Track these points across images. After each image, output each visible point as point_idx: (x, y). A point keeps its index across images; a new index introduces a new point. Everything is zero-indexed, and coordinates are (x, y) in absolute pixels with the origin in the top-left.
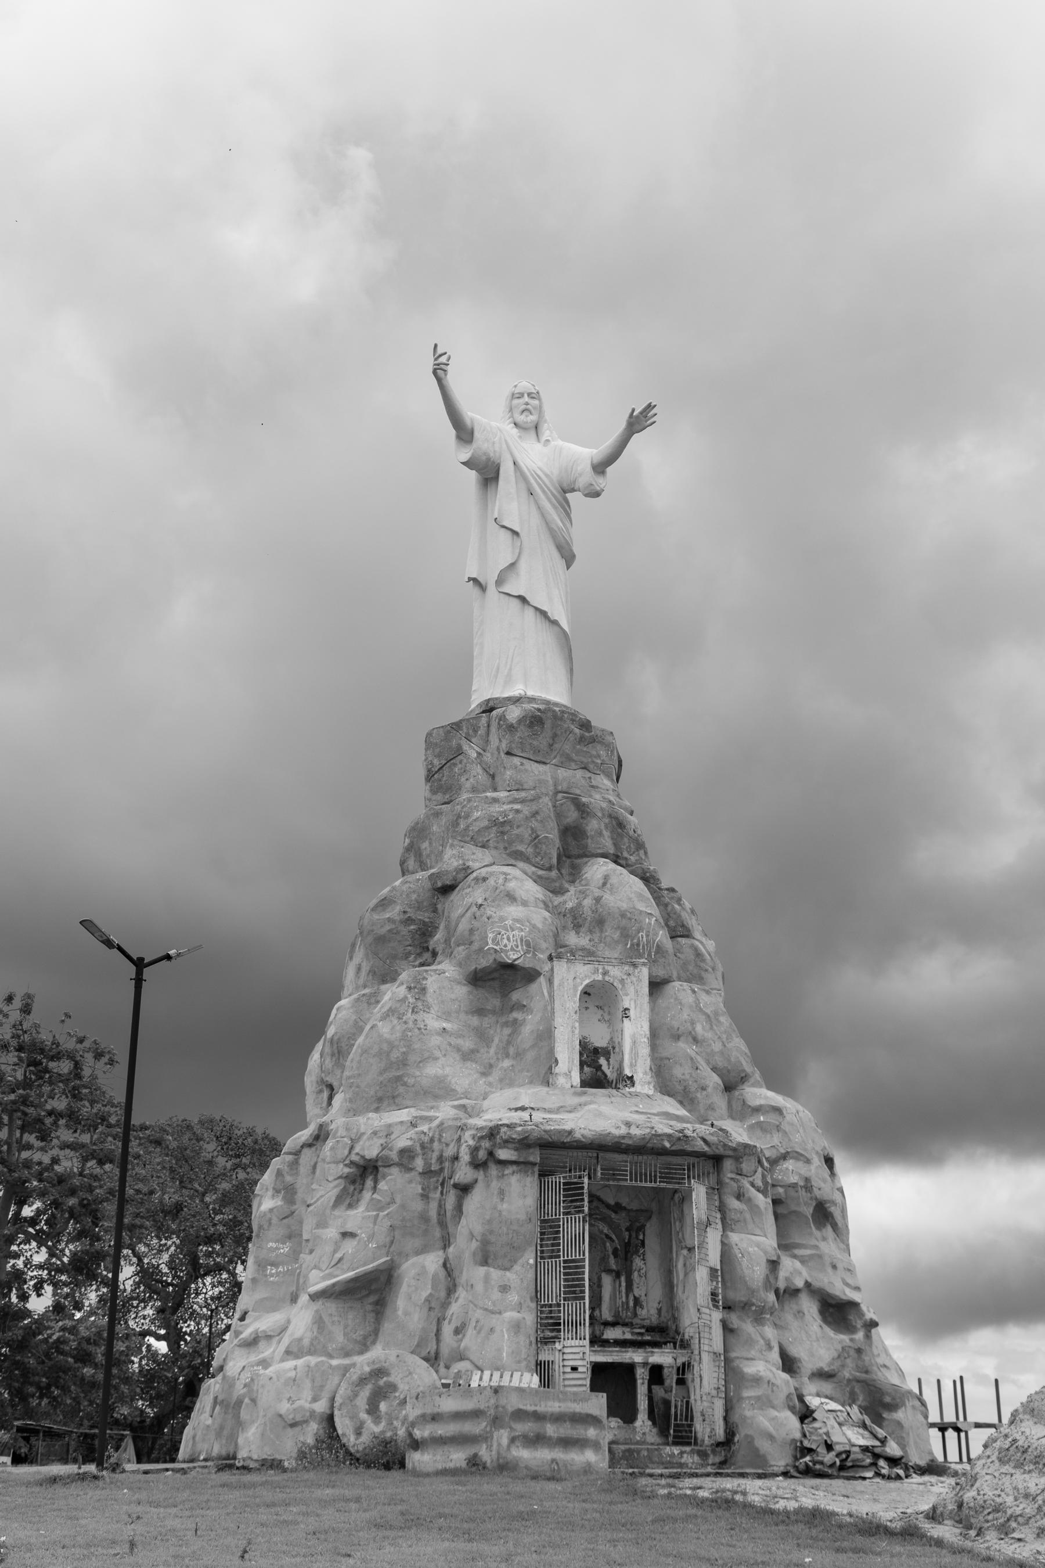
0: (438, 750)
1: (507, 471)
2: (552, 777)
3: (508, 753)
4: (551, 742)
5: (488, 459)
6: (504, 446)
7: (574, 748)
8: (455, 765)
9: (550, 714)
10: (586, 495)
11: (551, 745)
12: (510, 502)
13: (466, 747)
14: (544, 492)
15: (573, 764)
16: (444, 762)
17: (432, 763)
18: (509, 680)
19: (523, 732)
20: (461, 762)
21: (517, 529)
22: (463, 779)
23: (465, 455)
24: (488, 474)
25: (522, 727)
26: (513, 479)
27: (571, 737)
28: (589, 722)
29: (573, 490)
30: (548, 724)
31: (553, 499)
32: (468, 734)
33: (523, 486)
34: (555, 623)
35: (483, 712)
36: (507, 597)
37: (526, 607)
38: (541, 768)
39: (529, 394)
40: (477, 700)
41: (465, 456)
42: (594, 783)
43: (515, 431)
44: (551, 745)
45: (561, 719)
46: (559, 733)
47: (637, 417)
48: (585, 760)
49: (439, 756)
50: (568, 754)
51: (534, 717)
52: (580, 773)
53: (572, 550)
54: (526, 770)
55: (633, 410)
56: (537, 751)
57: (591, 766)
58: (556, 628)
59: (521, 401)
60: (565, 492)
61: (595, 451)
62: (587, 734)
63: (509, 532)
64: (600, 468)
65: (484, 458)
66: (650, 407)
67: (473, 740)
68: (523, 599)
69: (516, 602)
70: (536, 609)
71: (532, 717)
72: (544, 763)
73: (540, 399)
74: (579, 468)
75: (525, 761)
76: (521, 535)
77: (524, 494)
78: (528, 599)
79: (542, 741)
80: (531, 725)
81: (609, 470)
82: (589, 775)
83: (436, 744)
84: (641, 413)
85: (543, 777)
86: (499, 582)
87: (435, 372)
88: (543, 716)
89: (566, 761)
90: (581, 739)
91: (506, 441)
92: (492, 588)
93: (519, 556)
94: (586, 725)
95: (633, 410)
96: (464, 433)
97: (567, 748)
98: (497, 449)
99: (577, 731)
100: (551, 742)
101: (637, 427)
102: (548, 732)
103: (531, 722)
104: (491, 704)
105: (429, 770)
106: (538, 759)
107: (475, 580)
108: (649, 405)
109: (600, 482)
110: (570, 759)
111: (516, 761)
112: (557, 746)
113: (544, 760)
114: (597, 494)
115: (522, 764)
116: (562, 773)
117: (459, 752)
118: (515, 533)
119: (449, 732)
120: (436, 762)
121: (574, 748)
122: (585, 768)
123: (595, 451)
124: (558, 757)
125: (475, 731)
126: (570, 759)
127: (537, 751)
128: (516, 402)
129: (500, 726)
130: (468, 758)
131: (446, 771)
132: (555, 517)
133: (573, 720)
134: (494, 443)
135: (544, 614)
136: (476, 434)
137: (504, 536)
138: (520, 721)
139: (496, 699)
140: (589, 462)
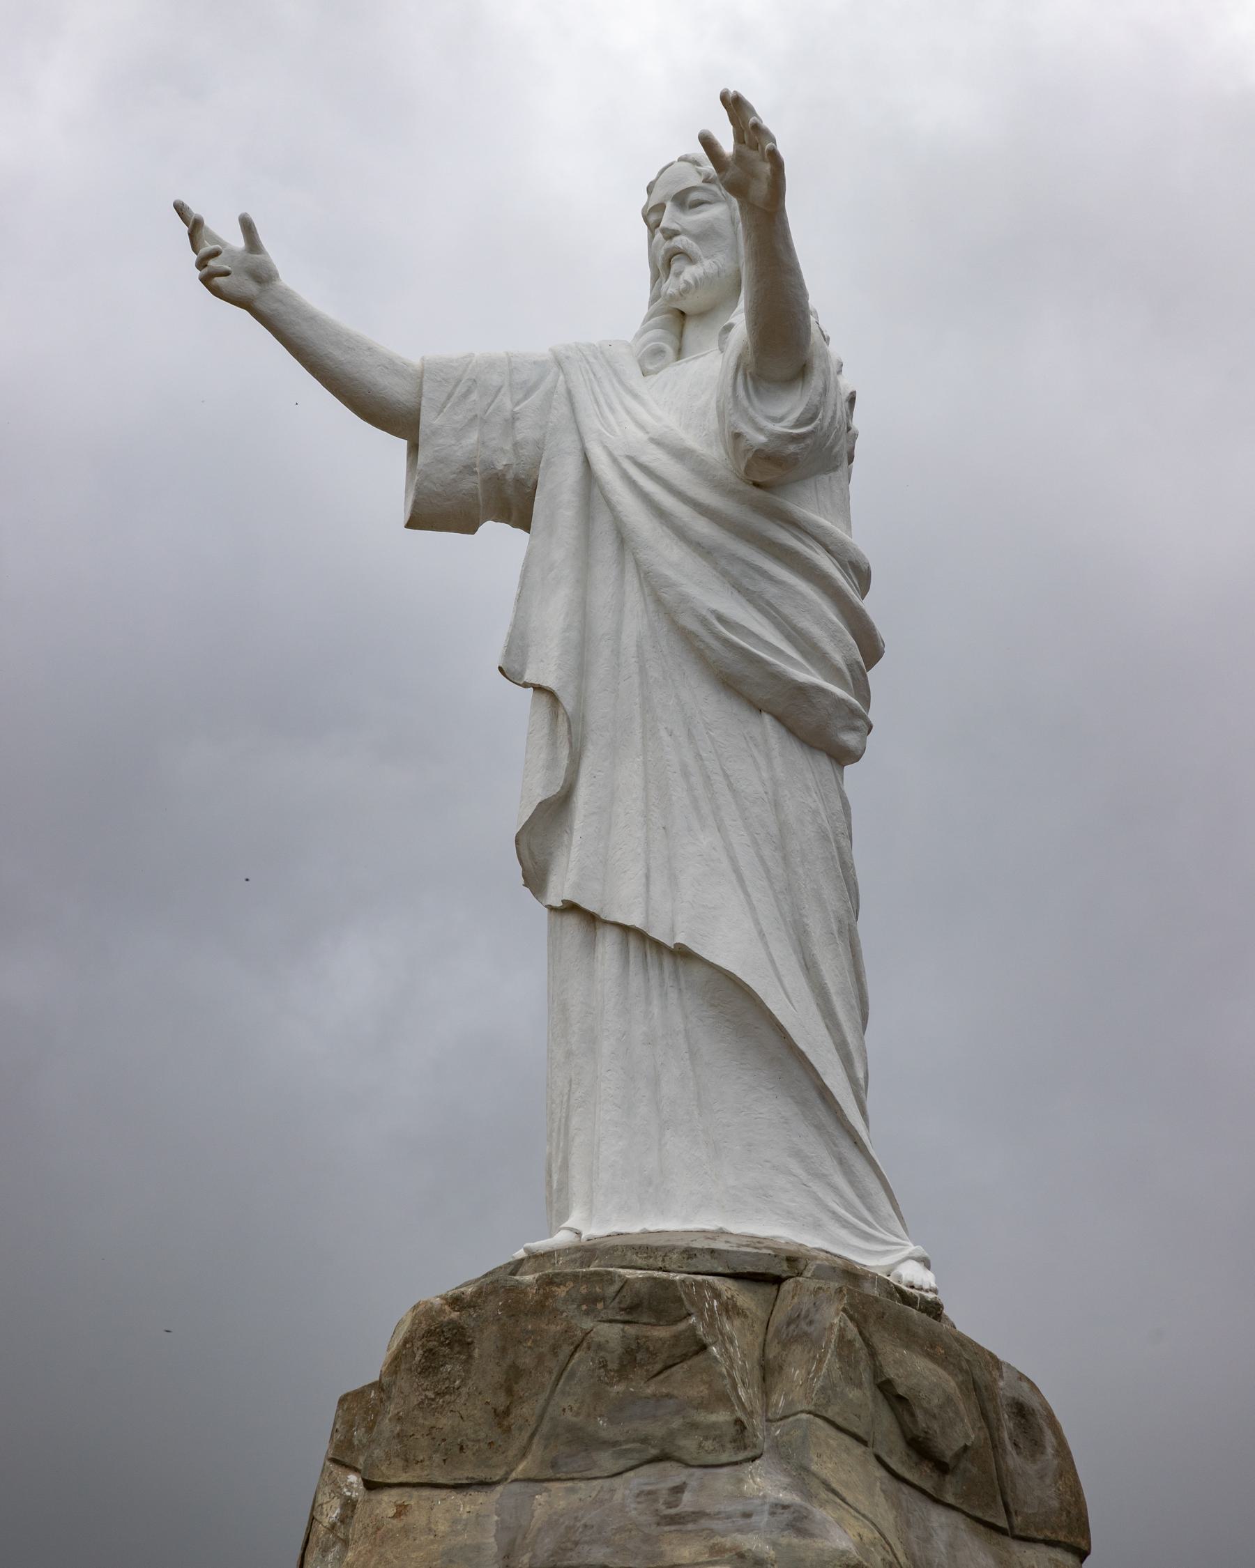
2: (502, 1527)
4: (501, 1401)
7: (598, 1396)
9: (494, 1306)
27: (583, 1363)
30: (485, 1344)
31: (702, 528)
38: (464, 1505)
42: (688, 1501)
46: (527, 1361)
48: (656, 1429)
54: (406, 1531)
56: (454, 1450)
57: (688, 1445)
62: (662, 1333)
71: (430, 1333)
75: (414, 1498)
79: (467, 1415)
85: (464, 1538)
89: (572, 1452)
90: (632, 1358)
97: (568, 1405)
103: (430, 1353)
106: (462, 1476)
110: (583, 1441)
112: (526, 1411)
113: (480, 1474)
116: (552, 1501)
124: (537, 1448)
127: (454, 1450)
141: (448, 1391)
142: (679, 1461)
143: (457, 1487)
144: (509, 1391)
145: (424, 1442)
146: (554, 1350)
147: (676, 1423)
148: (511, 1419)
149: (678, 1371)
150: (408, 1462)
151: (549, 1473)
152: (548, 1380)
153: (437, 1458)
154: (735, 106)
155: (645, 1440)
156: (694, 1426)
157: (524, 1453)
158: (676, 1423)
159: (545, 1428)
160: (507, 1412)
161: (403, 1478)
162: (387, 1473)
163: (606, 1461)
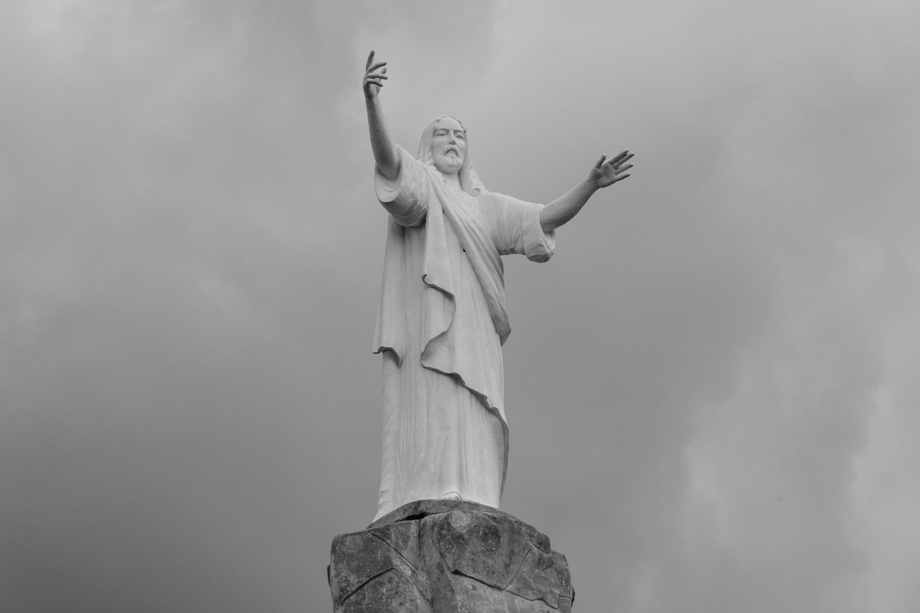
0: (355, 563)
1: (435, 218)
3: (457, 572)
4: (508, 561)
5: (415, 202)
6: (431, 189)
7: (532, 571)
8: (381, 584)
9: (506, 525)
10: (532, 258)
11: (507, 566)
12: (439, 255)
13: (396, 562)
14: (479, 249)
15: (530, 592)
16: (365, 579)
17: (347, 581)
18: (441, 481)
19: (475, 545)
20: (390, 581)
21: (451, 290)
22: (395, 604)
23: (388, 194)
24: (408, 222)
25: (474, 540)
26: (444, 230)
28: (547, 539)
29: (513, 251)
30: (504, 539)
31: (489, 261)
32: (397, 544)
33: (454, 239)
34: (493, 412)
35: (410, 518)
36: (435, 375)
37: (460, 389)
38: (496, 594)
39: (455, 132)
40: (387, 506)
41: (389, 197)
43: (439, 174)
44: (507, 566)
45: (519, 533)
46: (517, 551)
47: (606, 167)
48: (543, 588)
49: (357, 571)
50: (525, 579)
51: (489, 528)
52: (538, 604)
53: (508, 325)
54: (480, 597)
55: (604, 159)
56: (491, 572)
58: (494, 419)
59: (445, 139)
60: (500, 253)
61: (541, 206)
62: (545, 555)
63: (440, 295)
64: (551, 225)
65: (411, 200)
66: (624, 156)
67: (404, 553)
68: (456, 378)
69: (448, 383)
70: (472, 392)
72: (499, 589)
73: (465, 139)
74: (524, 225)
75: (477, 584)
76: (457, 298)
77: (456, 250)
78: (464, 377)
79: (498, 561)
80: (484, 539)
81: (557, 230)
82: (547, 608)
83: (352, 556)
84: (612, 163)
86: (425, 355)
87: (367, 88)
88: (499, 527)
89: (524, 588)
91: (433, 183)
92: (412, 361)
93: (451, 325)
94: (544, 543)
95: (604, 159)
96: (387, 164)
98: (424, 191)
99: (535, 550)
100: (508, 561)
101: (604, 180)
102: (504, 550)
103: (485, 534)
104: (422, 508)
105: (342, 590)
106: (492, 582)
107: (388, 352)
108: (625, 154)
109: (550, 244)
110: (528, 586)
111: (467, 583)
112: (513, 567)
113: (499, 585)
114: (543, 258)
115: (474, 588)
116: (519, 602)
117: (388, 567)
118: (448, 296)
119: (370, 541)
120: (353, 579)
121: (532, 571)
122: (541, 599)
123: (541, 206)
125: (405, 542)
126: (528, 586)
127: (491, 572)
128: (439, 139)
129: (441, 537)
130: (401, 575)
131: (368, 591)
132: (490, 278)
133: (531, 536)
134: (421, 184)
135: (481, 399)
136: (405, 170)
137: (435, 298)
138: (471, 532)
139: (429, 501)
140: (538, 218)
141: (491, 550)
142: (546, 602)
143: (489, 586)
144: (510, 559)
145: (481, 566)
146: (524, 549)
147: (548, 589)
148: (509, 569)
149: (548, 570)
150: (474, 571)
151: (517, 592)
152: (521, 559)
153: (485, 573)
154: (632, 155)
155: (539, 591)
156: (552, 592)
157: (511, 583)
158: (548, 589)
159: (518, 576)
160: (508, 566)
161: (473, 575)
162: (465, 570)
163: (531, 595)
